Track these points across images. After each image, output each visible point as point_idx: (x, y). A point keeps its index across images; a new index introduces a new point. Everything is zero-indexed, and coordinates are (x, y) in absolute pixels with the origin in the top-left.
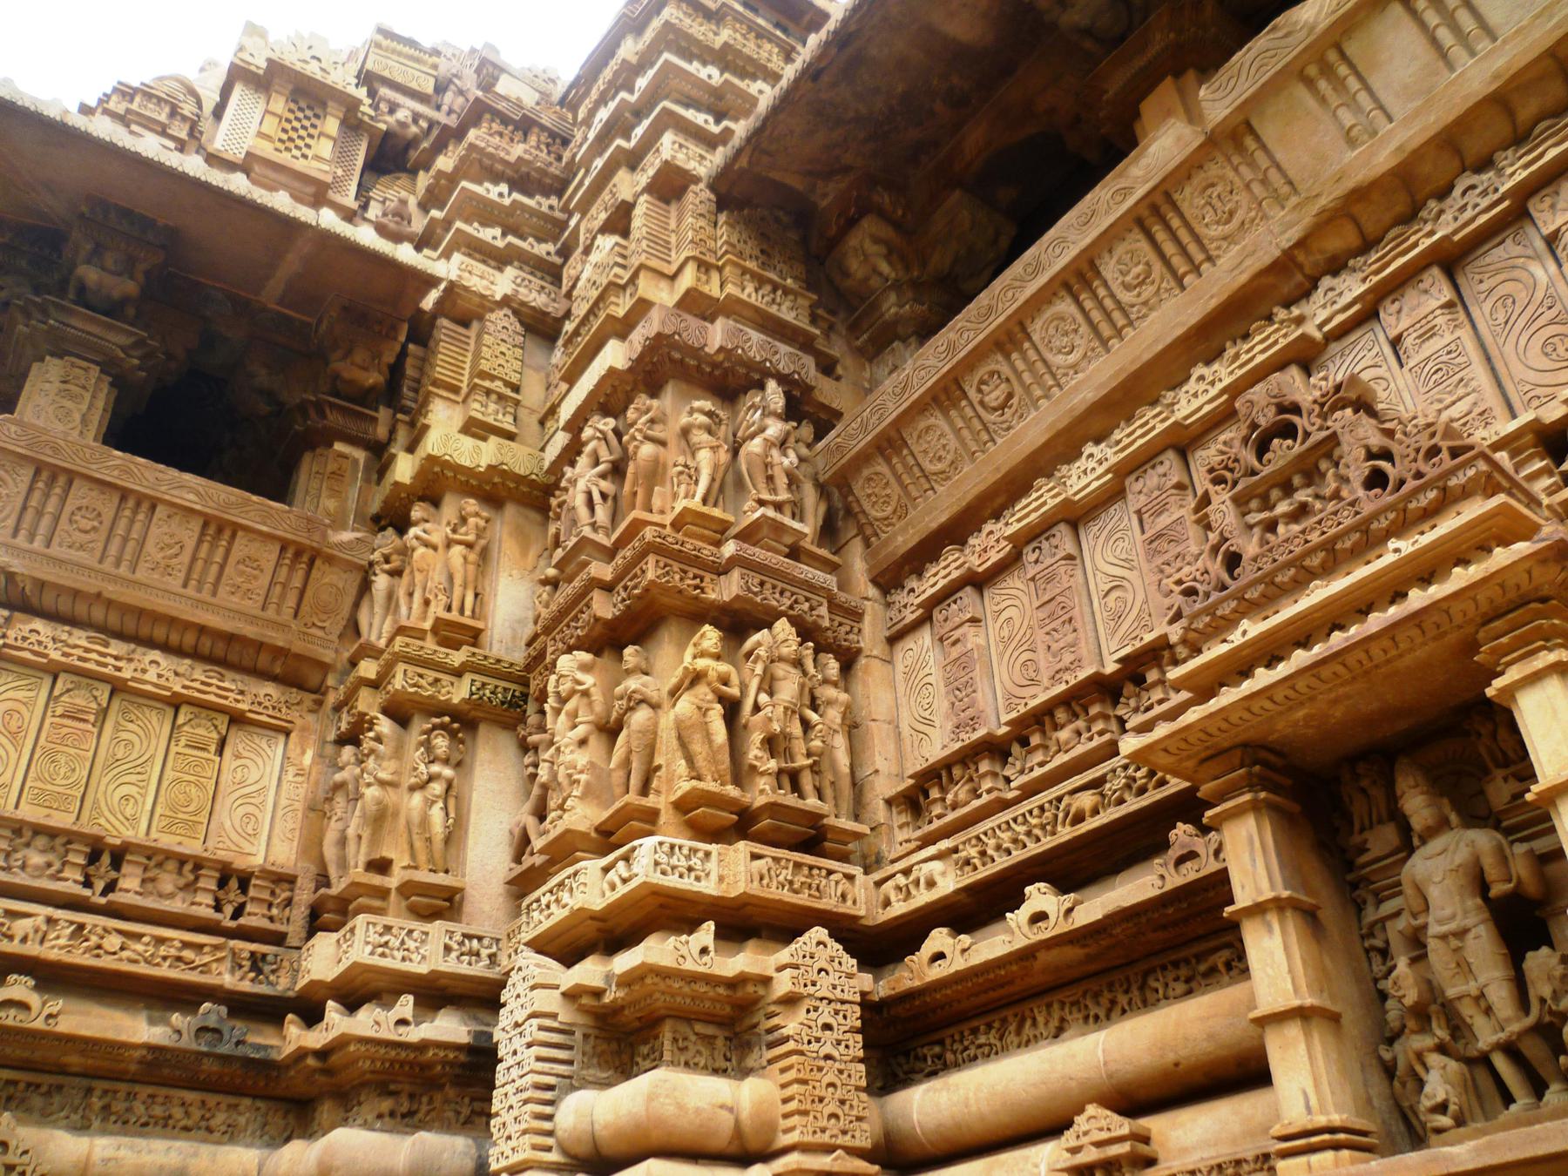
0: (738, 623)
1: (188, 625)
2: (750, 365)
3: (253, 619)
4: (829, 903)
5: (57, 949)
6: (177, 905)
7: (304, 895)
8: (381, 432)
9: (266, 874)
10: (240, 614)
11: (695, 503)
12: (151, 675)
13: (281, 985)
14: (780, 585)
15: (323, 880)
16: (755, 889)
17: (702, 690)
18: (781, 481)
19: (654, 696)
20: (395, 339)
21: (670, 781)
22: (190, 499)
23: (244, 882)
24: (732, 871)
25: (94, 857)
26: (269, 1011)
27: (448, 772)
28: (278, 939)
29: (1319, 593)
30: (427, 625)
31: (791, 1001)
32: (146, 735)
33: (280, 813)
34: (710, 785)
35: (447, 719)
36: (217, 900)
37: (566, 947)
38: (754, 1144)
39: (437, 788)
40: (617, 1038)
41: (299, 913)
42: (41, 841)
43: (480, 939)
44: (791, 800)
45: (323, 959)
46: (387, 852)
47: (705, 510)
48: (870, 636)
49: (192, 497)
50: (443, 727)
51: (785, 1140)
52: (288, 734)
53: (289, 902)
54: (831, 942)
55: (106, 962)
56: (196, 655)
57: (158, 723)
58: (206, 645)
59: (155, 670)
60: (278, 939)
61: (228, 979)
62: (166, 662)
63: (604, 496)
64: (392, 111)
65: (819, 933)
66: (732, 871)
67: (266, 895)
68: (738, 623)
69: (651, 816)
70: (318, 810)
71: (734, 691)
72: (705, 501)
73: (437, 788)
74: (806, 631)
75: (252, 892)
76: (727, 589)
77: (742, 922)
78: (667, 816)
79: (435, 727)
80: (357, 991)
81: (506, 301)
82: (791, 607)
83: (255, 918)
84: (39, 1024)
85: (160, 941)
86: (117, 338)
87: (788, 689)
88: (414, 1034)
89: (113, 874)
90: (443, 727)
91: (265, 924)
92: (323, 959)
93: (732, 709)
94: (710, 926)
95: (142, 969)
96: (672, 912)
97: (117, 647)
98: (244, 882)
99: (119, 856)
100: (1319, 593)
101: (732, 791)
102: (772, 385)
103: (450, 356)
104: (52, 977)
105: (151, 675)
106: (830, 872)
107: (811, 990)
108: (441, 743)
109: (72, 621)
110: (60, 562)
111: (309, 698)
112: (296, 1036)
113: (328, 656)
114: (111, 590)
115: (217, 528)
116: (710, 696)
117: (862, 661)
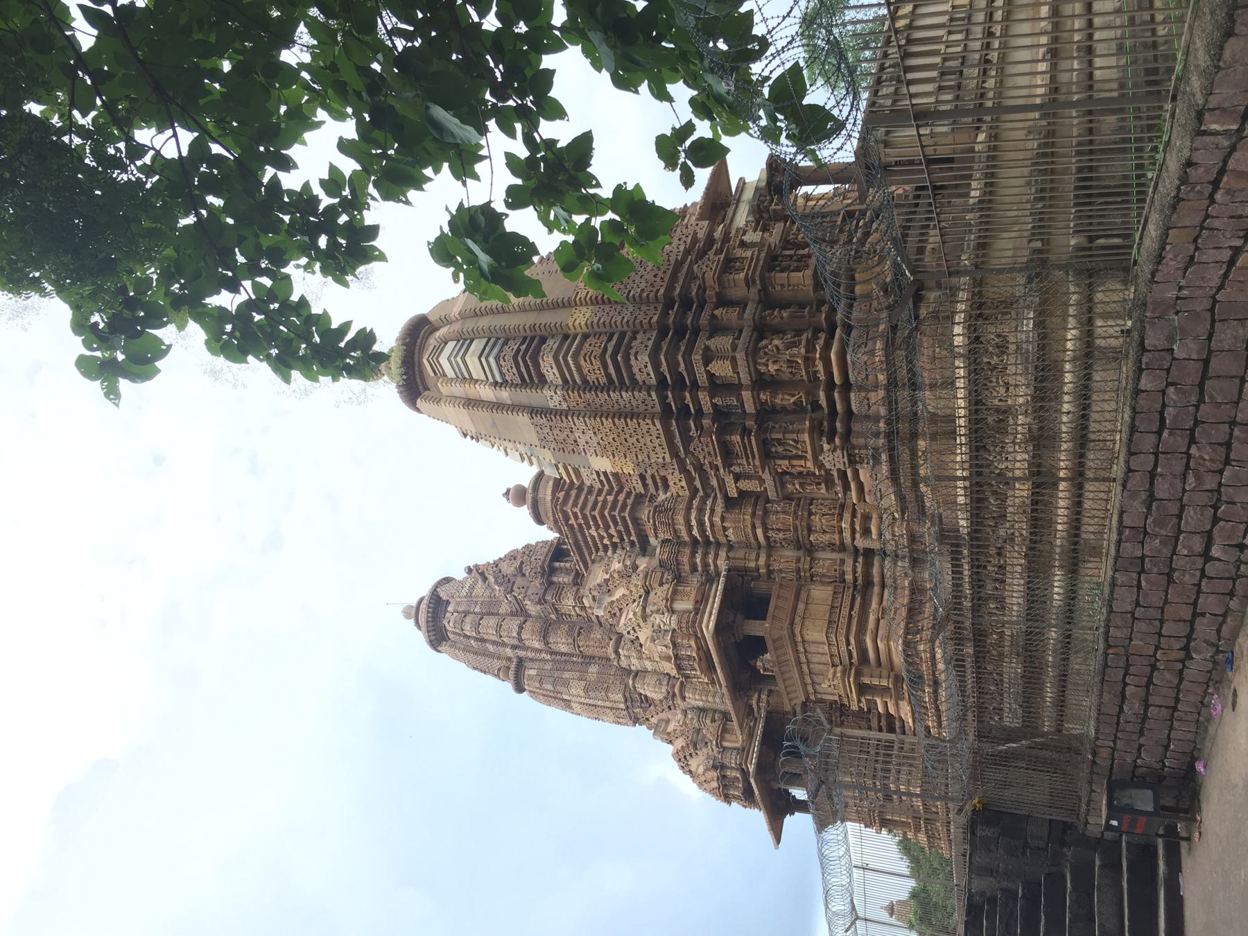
0: (810, 514)
24: (847, 516)
32: (812, 607)
40: (866, 532)
45: (849, 577)
59: (801, 606)
66: (847, 516)
68: (810, 514)
70: (823, 583)
76: (806, 514)
77: (854, 516)
80: (855, 572)
92: (849, 577)
96: (853, 523)
103: (740, 564)
104: (852, 609)
112: (860, 581)
115: (778, 597)
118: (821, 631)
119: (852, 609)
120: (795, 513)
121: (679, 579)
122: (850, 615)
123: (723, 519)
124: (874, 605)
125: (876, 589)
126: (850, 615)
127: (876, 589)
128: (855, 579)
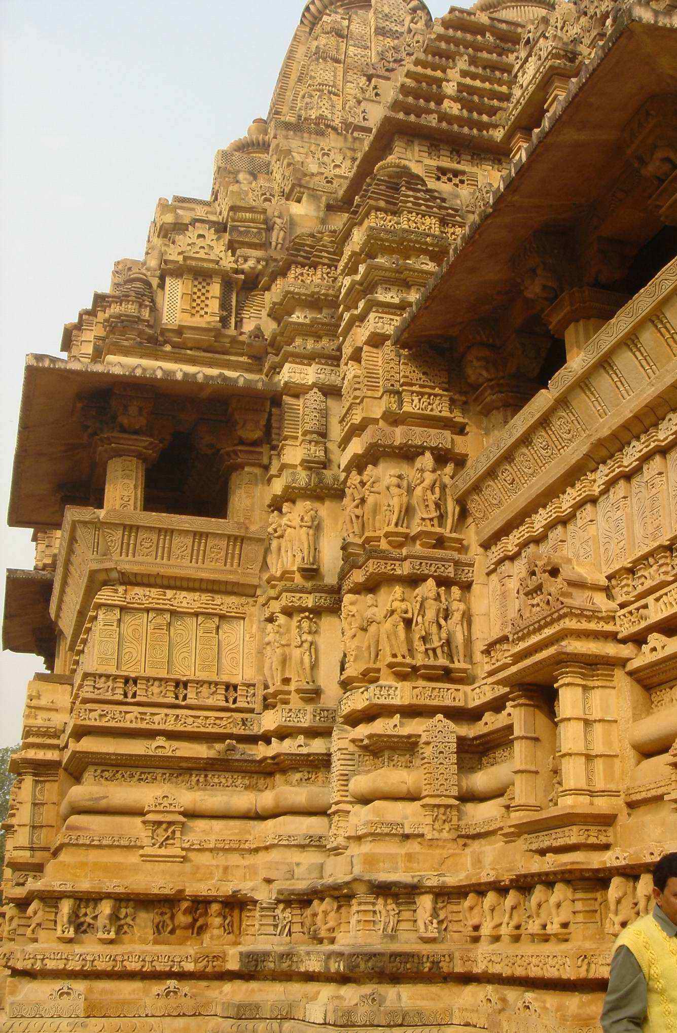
1: (195, 580)
2: (416, 447)
3: (222, 572)
4: (448, 702)
5: (170, 726)
6: (210, 702)
7: (260, 692)
8: (265, 461)
9: (244, 684)
10: (215, 570)
11: (391, 528)
12: (184, 604)
13: (256, 730)
14: (429, 562)
15: (266, 687)
16: (415, 701)
17: (396, 616)
18: (432, 507)
19: (378, 619)
20: (265, 411)
21: (384, 657)
22: (186, 527)
23: (235, 687)
25: (177, 686)
26: (253, 740)
27: (310, 638)
28: (251, 711)
29: (548, 632)
30: (295, 568)
31: (428, 743)
32: (187, 629)
33: (245, 656)
34: (399, 659)
35: (307, 614)
36: (226, 697)
37: (354, 719)
38: (415, 795)
39: (306, 645)
41: (259, 698)
42: (157, 683)
43: (328, 711)
44: (431, 662)
45: (270, 721)
46: (287, 675)
47: (396, 530)
48: (477, 574)
49: (187, 525)
50: (307, 617)
51: (424, 793)
52: (244, 619)
53: (254, 695)
54: (443, 719)
55: (189, 729)
56: (201, 590)
57: (191, 622)
58: (204, 586)
60: (251, 711)
61: (235, 731)
62: (190, 596)
63: (357, 517)
64: (246, 261)
65: (440, 716)
67: (245, 693)
69: (378, 670)
71: (409, 615)
72: (396, 525)
73: (306, 645)
74: (444, 582)
75: (239, 692)
76: (405, 569)
77: (411, 712)
78: (385, 671)
79: (303, 618)
80: (283, 734)
81: (314, 385)
82: (435, 571)
83: (241, 704)
84: (170, 754)
85: (207, 718)
86: (143, 443)
87: (430, 614)
88: (304, 750)
89: (185, 692)
90: (307, 617)
91: (246, 705)
93: (408, 623)
94: (398, 715)
95: (202, 730)
97: (170, 593)
98: (235, 687)
99: (185, 685)
100: (534, 639)
101: (408, 660)
102: (428, 454)
104: (172, 736)
105: (185, 601)
106: (448, 689)
107: (435, 739)
108: (305, 624)
109: (149, 585)
110: (141, 563)
111: (251, 600)
113: (255, 581)
114: (162, 571)
116: (399, 619)
117: (474, 586)
118: (103, 661)
119: (172, 736)
120: (410, 539)
121: (242, 287)
122: (151, 734)
123: (377, 341)
124: (186, 796)
125: (243, 800)
126: (151, 734)
127: (243, 800)
128: (266, 738)
